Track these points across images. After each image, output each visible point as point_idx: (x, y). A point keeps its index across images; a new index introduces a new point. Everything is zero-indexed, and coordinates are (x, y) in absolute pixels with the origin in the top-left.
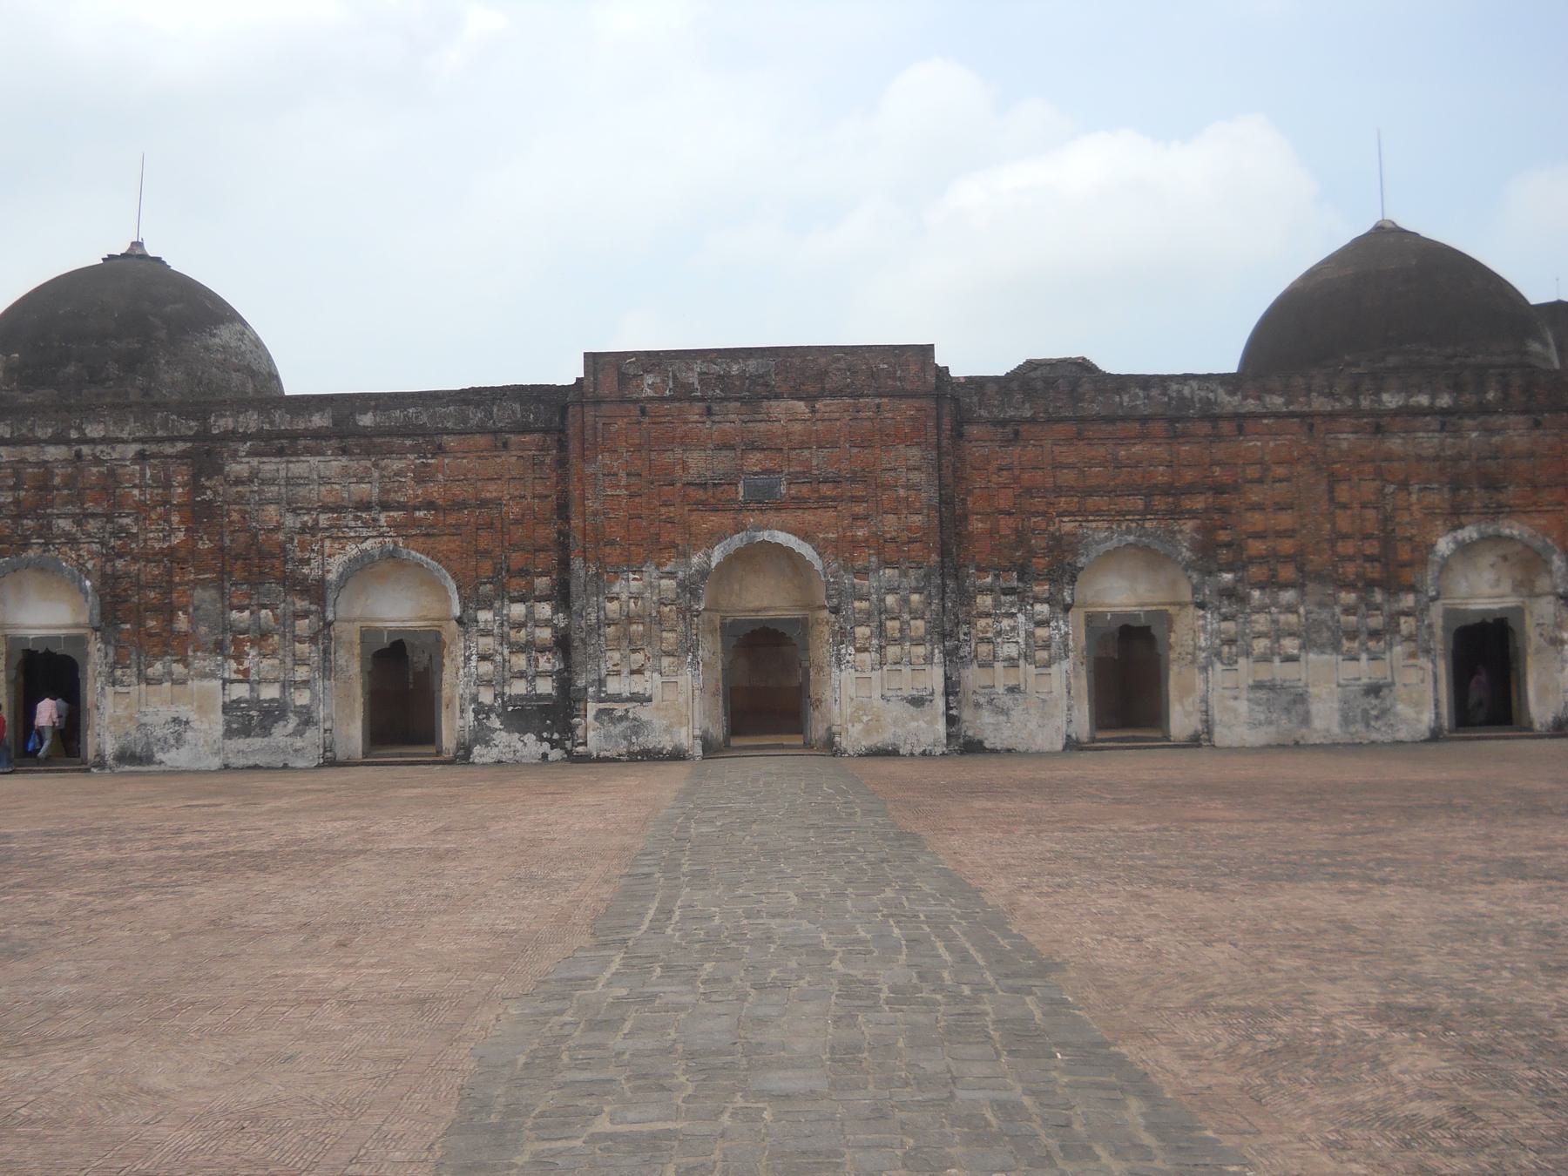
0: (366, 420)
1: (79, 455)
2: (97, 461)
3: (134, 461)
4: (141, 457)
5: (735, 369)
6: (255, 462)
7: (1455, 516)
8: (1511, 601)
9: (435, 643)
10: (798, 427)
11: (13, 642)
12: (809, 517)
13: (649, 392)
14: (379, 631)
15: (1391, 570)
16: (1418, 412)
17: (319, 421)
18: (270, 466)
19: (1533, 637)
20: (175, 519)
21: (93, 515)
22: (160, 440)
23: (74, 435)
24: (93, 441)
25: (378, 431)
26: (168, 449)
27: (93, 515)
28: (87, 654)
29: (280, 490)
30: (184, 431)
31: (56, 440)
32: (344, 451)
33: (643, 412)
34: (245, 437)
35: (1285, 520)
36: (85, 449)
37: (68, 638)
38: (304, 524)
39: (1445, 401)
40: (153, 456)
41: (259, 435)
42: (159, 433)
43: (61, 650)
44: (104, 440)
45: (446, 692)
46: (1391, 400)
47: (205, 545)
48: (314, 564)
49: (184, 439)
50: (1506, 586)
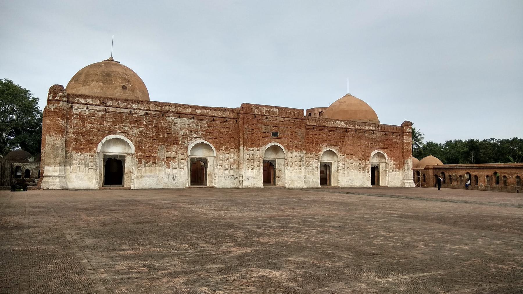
0: (198, 111)
1: (131, 112)
2: (136, 114)
3: (144, 115)
4: (147, 114)
5: (271, 110)
6: (173, 118)
7: (374, 148)
8: (378, 164)
9: (206, 161)
10: (281, 123)
11: (105, 156)
12: (282, 140)
13: (256, 113)
14: (194, 158)
15: (367, 157)
16: (370, 130)
17: (188, 110)
18: (176, 120)
19: (381, 170)
20: (154, 129)
21: (134, 127)
22: (152, 111)
23: (129, 106)
24: (134, 109)
25: (200, 115)
26: (153, 113)
27: (134, 127)
28: (124, 160)
29: (180, 125)
30: (157, 109)
31: (126, 107)
32: (193, 118)
33: (255, 117)
34: (171, 112)
35: (351, 147)
36: (132, 110)
37: (121, 156)
38: (184, 133)
39: (374, 129)
40: (150, 114)
41: (174, 112)
42: (151, 109)
43: (118, 159)
44: (137, 109)
45: (208, 172)
46: (367, 128)
47: (161, 136)
48: (186, 142)
49: (158, 111)
50: (378, 161)
